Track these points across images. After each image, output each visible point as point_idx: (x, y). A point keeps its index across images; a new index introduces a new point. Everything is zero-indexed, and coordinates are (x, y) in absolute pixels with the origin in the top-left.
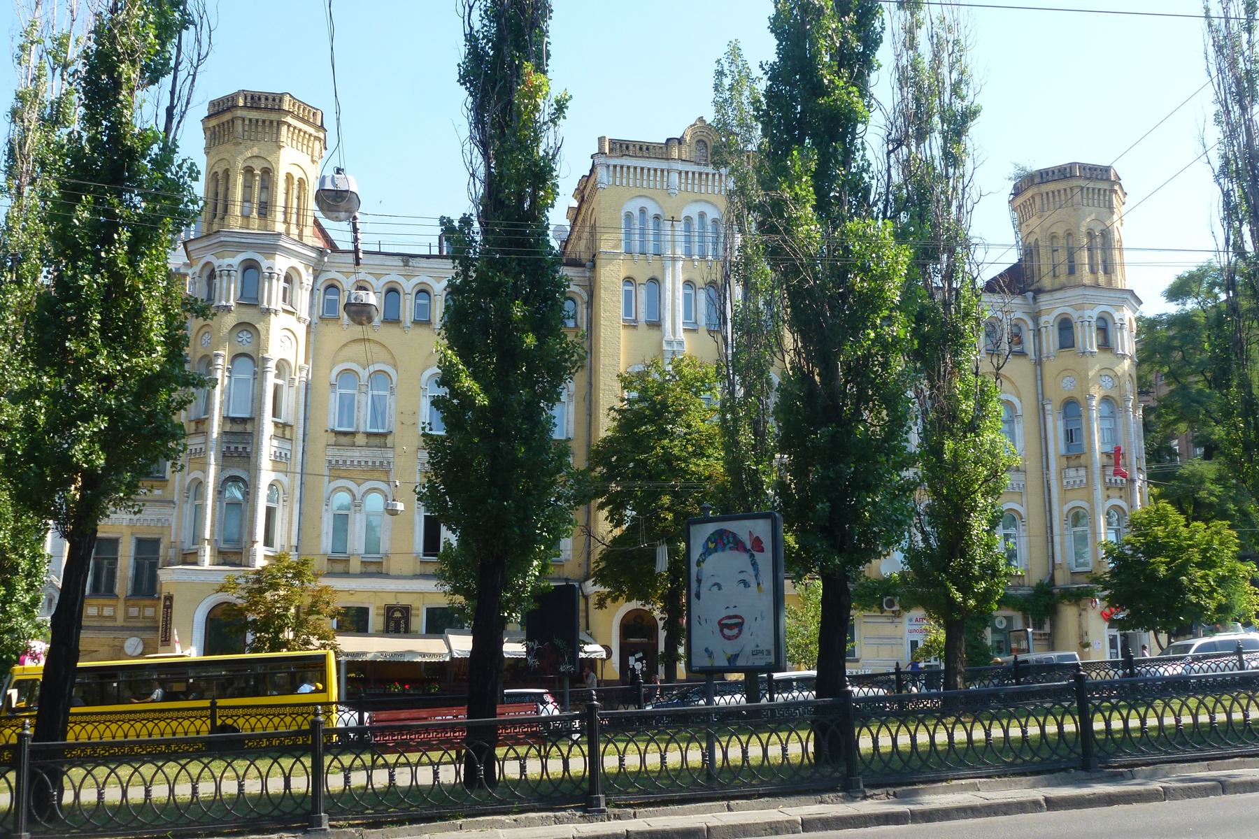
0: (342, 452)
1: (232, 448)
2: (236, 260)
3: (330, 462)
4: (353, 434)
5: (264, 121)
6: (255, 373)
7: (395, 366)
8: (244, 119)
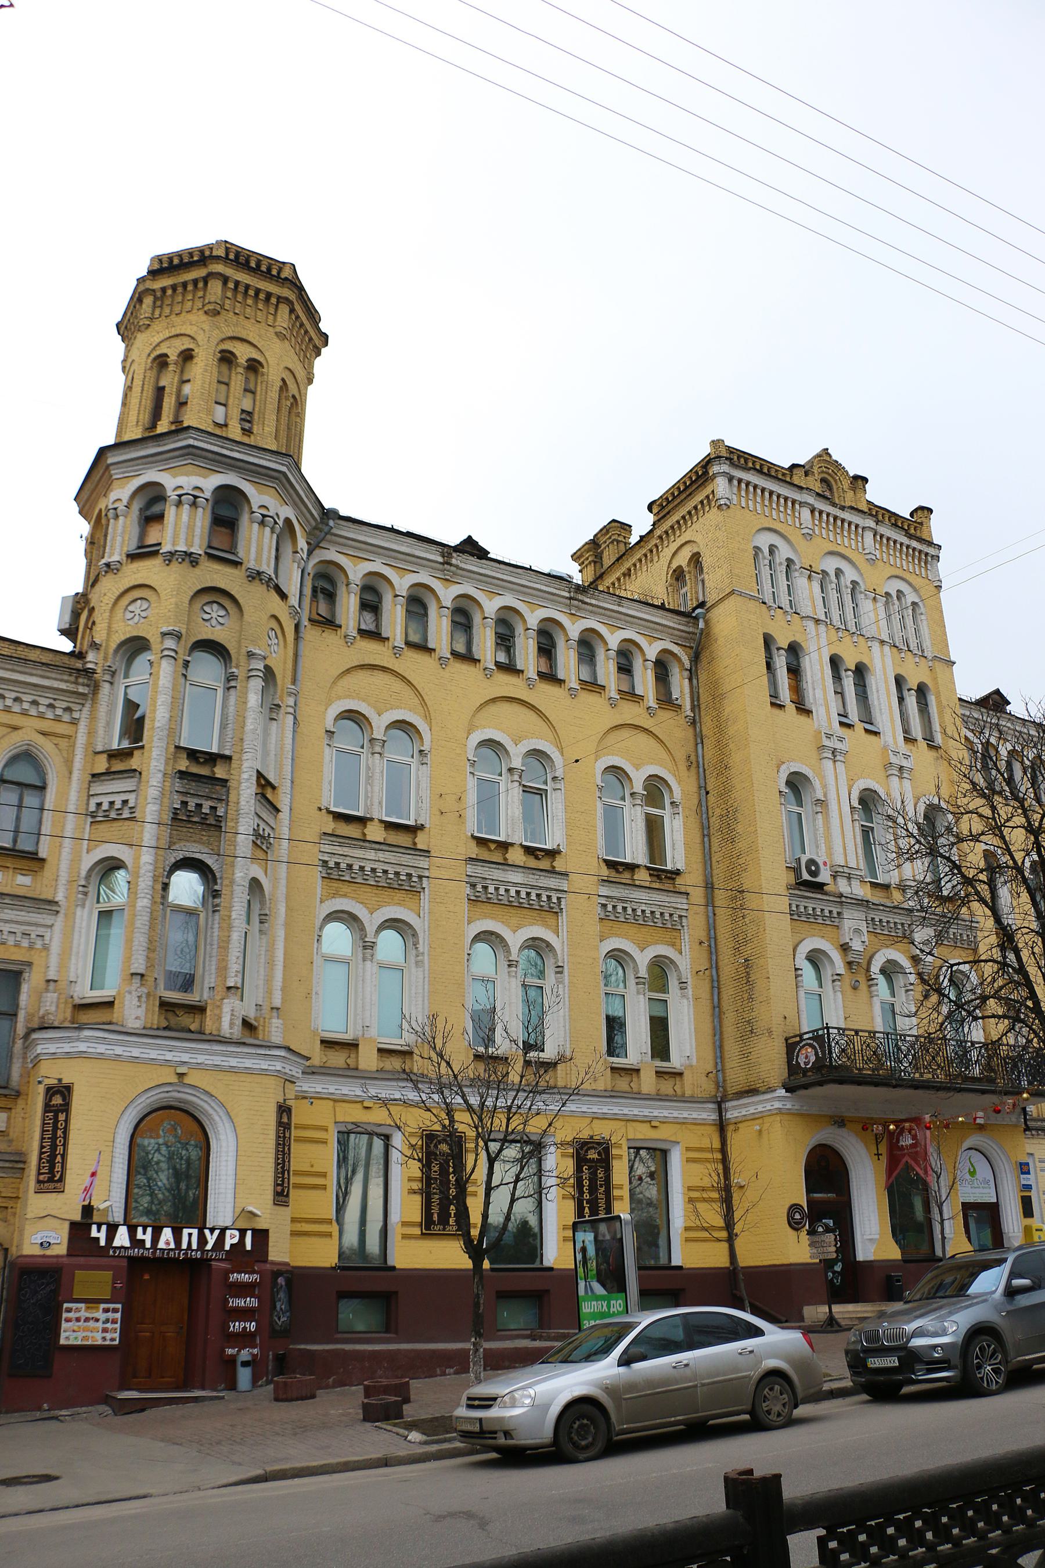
1: (191, 806)
2: (210, 482)
4: (362, 821)
6: (230, 678)
7: (427, 717)
8: (225, 280)
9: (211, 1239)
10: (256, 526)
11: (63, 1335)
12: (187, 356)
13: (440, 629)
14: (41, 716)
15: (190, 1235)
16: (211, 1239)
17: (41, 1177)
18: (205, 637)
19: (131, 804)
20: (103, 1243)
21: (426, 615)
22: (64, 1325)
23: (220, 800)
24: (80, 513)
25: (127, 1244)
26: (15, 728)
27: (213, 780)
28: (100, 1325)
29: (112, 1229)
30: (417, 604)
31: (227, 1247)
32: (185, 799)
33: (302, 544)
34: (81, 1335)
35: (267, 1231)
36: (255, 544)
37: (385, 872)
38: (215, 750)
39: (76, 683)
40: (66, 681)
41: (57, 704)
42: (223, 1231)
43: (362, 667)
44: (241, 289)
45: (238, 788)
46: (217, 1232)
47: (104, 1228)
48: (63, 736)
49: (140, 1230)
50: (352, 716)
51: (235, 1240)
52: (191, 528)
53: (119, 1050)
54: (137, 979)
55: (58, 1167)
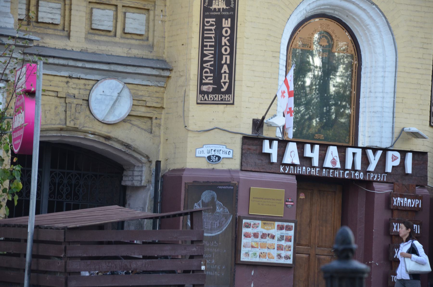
9: (374, 160)
11: (243, 250)
15: (354, 154)
16: (374, 160)
17: (205, 88)
20: (274, 159)
22: (244, 241)
25: (297, 161)
28: (275, 242)
29: (283, 144)
31: (389, 169)
34: (258, 251)
35: (426, 153)
42: (385, 151)
46: (379, 153)
47: (275, 143)
49: (308, 147)
51: (397, 163)
55: (225, 78)
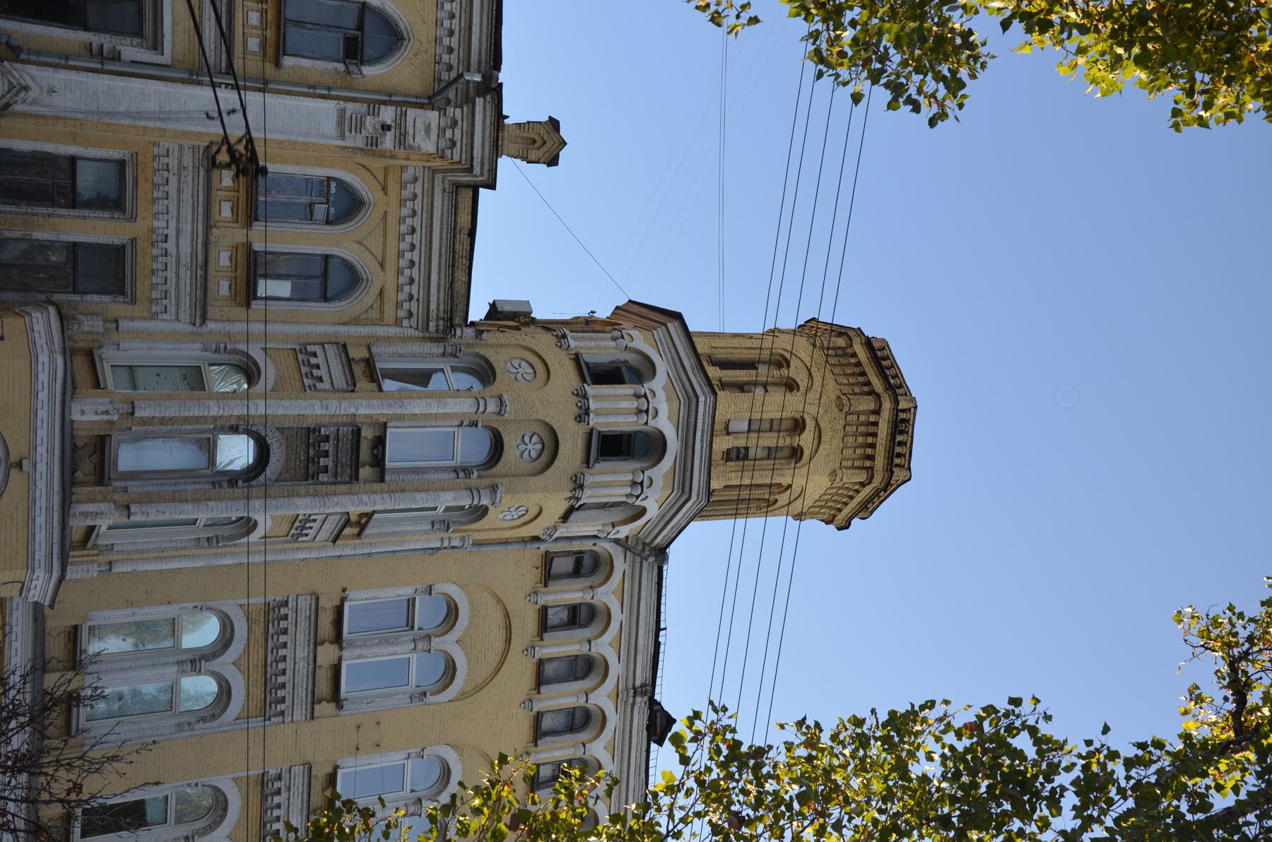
0: (303, 624)
1: (325, 446)
2: (665, 424)
3: (286, 603)
4: (338, 639)
5: (873, 446)
6: (467, 471)
7: (463, 696)
8: (877, 412)
10: (630, 477)
12: (791, 386)
13: (563, 697)
14: (399, 288)
18: (505, 440)
19: (319, 385)
21: (576, 679)
23: (336, 475)
24: (617, 308)
26: (382, 265)
27: (356, 466)
30: (585, 667)
32: (331, 438)
33: (624, 531)
36: (611, 481)
37: (284, 672)
38: (388, 464)
39: (438, 319)
40: (438, 309)
41: (414, 303)
43: (507, 616)
44: (871, 429)
45: (351, 493)
48: (382, 312)
50: (452, 612)
52: (615, 412)
53: (43, 395)
54: (127, 408)
